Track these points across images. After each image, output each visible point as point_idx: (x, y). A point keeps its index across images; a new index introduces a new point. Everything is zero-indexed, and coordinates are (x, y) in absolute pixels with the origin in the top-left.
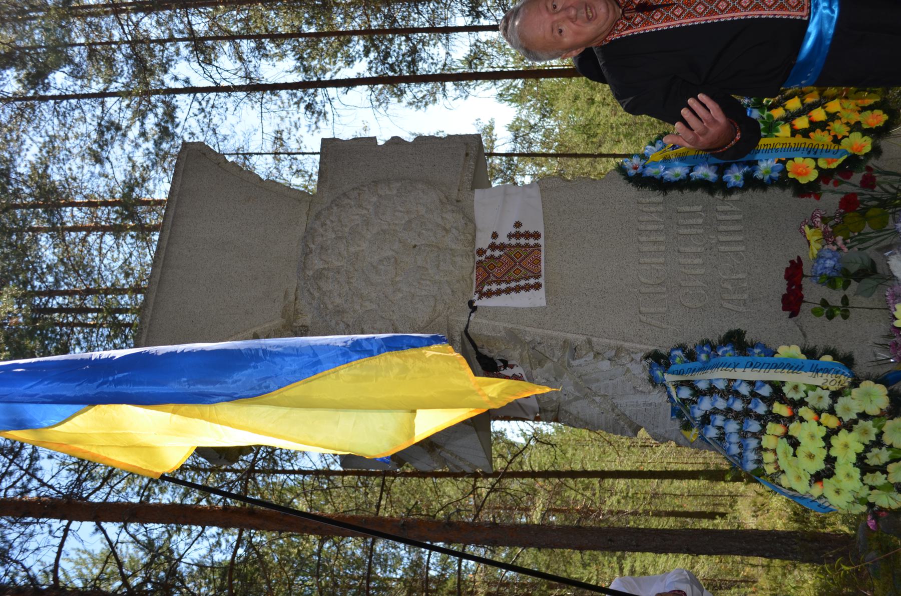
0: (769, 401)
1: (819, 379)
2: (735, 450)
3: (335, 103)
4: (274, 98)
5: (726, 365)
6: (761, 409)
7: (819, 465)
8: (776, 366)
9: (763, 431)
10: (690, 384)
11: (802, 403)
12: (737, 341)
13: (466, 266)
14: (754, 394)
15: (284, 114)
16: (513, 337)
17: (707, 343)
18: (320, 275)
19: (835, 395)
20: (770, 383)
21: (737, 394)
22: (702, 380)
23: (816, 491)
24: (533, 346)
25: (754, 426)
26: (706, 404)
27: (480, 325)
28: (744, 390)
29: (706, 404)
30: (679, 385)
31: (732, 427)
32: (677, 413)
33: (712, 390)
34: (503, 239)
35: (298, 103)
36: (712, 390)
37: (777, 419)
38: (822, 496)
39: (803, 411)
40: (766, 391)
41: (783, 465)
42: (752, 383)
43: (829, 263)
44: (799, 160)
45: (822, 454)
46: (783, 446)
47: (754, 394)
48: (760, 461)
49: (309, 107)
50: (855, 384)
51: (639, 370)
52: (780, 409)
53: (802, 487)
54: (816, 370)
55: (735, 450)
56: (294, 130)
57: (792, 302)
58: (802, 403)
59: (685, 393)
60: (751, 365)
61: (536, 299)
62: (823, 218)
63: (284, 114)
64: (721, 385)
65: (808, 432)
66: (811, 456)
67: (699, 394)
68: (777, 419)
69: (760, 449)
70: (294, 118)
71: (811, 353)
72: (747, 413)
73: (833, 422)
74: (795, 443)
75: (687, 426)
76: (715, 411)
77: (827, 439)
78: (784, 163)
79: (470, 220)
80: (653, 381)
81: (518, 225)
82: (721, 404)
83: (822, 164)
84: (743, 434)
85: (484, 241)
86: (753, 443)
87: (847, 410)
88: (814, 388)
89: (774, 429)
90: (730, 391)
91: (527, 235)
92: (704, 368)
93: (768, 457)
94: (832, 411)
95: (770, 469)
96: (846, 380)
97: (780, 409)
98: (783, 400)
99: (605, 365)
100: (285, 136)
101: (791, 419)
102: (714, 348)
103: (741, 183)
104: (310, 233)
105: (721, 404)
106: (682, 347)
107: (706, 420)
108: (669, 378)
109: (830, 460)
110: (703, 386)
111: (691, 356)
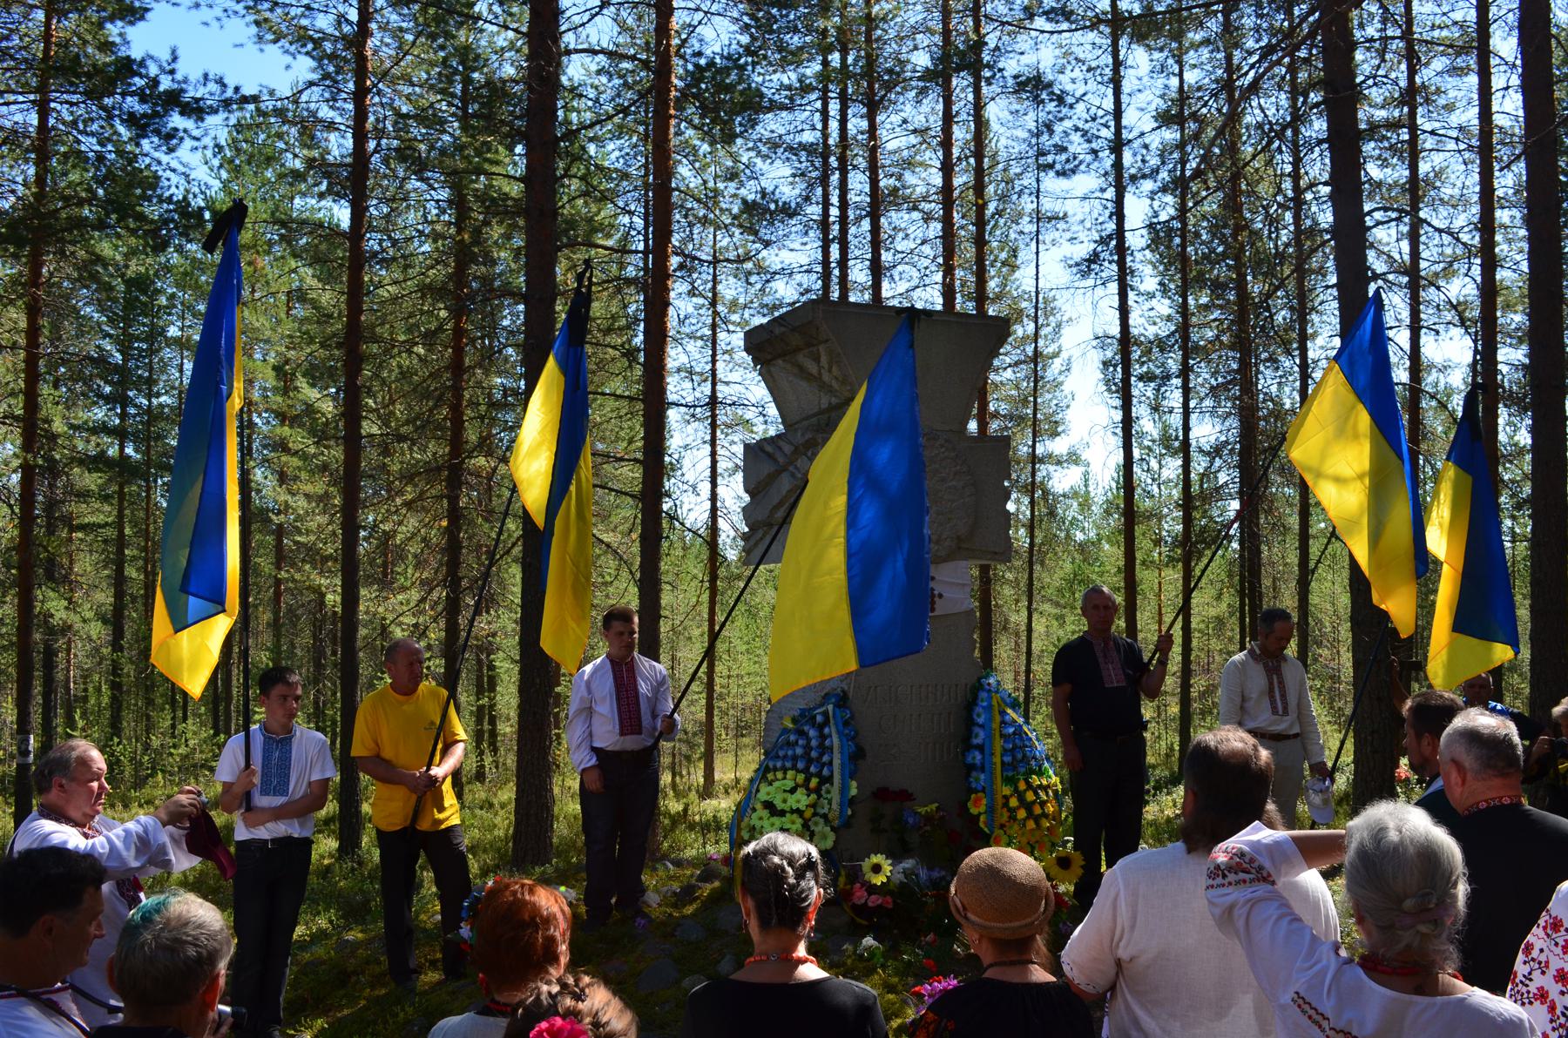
0: (819, 775)
1: (835, 806)
2: (781, 753)
3: (1100, 291)
4: (1107, 213)
5: (842, 747)
6: (812, 769)
7: (780, 805)
8: (843, 779)
9: (798, 771)
10: (826, 722)
11: (820, 796)
12: (856, 756)
14: (823, 765)
15: (1088, 225)
17: (857, 733)
19: (825, 816)
20: (831, 776)
21: (821, 755)
22: (831, 730)
23: (759, 806)
25: (800, 765)
28: (825, 758)
29: (812, 733)
30: (825, 714)
31: (799, 751)
32: (803, 712)
33: (823, 737)
34: (932, 584)
36: (823, 737)
37: (807, 780)
38: (754, 810)
39: (814, 796)
40: (825, 772)
41: (777, 784)
42: (831, 763)
43: (911, 820)
44: (984, 802)
45: (786, 807)
46: (789, 784)
47: (823, 765)
48: (775, 769)
49: (1096, 254)
50: (833, 829)
52: (814, 782)
53: (762, 796)
54: (841, 804)
55: (781, 753)
56: (1068, 235)
57: (882, 794)
58: (820, 796)
59: (819, 719)
60: (842, 764)
62: (942, 817)
64: (827, 742)
65: (801, 800)
66: (785, 801)
67: (821, 727)
68: (807, 780)
69: (785, 770)
70: (1082, 236)
71: (852, 802)
72: (810, 761)
73: (808, 814)
74: (793, 791)
75: (794, 720)
76: (809, 740)
77: (798, 812)
78: (983, 790)
79: (945, 560)
80: (826, 698)
81: (940, 596)
82: (814, 743)
83: (982, 818)
84: (795, 758)
86: (788, 764)
87: (816, 824)
88: (830, 803)
89: (801, 778)
90: (824, 749)
91: (933, 603)
92: (838, 732)
93: (779, 775)
94: (815, 814)
95: (770, 776)
96: (836, 823)
97: (814, 782)
98: (820, 784)
100: (1061, 225)
101: (807, 789)
102: (853, 739)
103: (969, 760)
105: (814, 743)
106: (852, 717)
108: (830, 707)
109: (782, 813)
110: (826, 730)
111: (846, 723)
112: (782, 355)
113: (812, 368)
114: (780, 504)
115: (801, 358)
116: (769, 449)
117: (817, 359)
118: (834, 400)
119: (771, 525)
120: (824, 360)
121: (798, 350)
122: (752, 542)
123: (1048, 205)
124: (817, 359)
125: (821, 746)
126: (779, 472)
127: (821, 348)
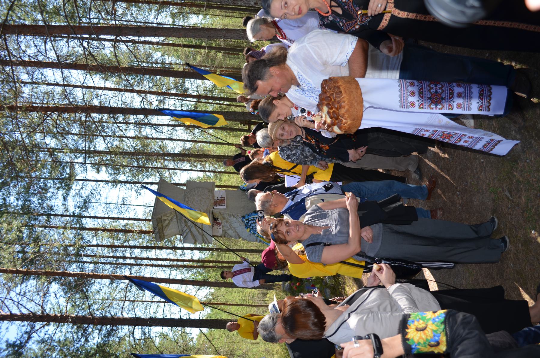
13: (213, 201)
16: (220, 213)
18: (187, 202)
24: (223, 214)
26: (250, 223)
27: (215, 211)
29: (250, 223)
33: (251, 220)
35: (131, 189)
51: (240, 220)
56: (129, 197)
61: (224, 207)
63: (127, 192)
67: (249, 221)
70: (129, 194)
75: (248, 228)
82: (252, 222)
85: (216, 198)
99: (235, 219)
104: (185, 195)
105: (252, 222)
107: (250, 225)
112: (163, 230)
113: (167, 222)
114: (198, 231)
115: (164, 225)
116: (185, 235)
117: (165, 220)
118: (175, 217)
119: (203, 235)
120: (166, 218)
121: (162, 225)
122: (207, 241)
123: (120, 202)
124: (165, 220)
125: (253, 220)
126: (191, 232)
127: (163, 218)
